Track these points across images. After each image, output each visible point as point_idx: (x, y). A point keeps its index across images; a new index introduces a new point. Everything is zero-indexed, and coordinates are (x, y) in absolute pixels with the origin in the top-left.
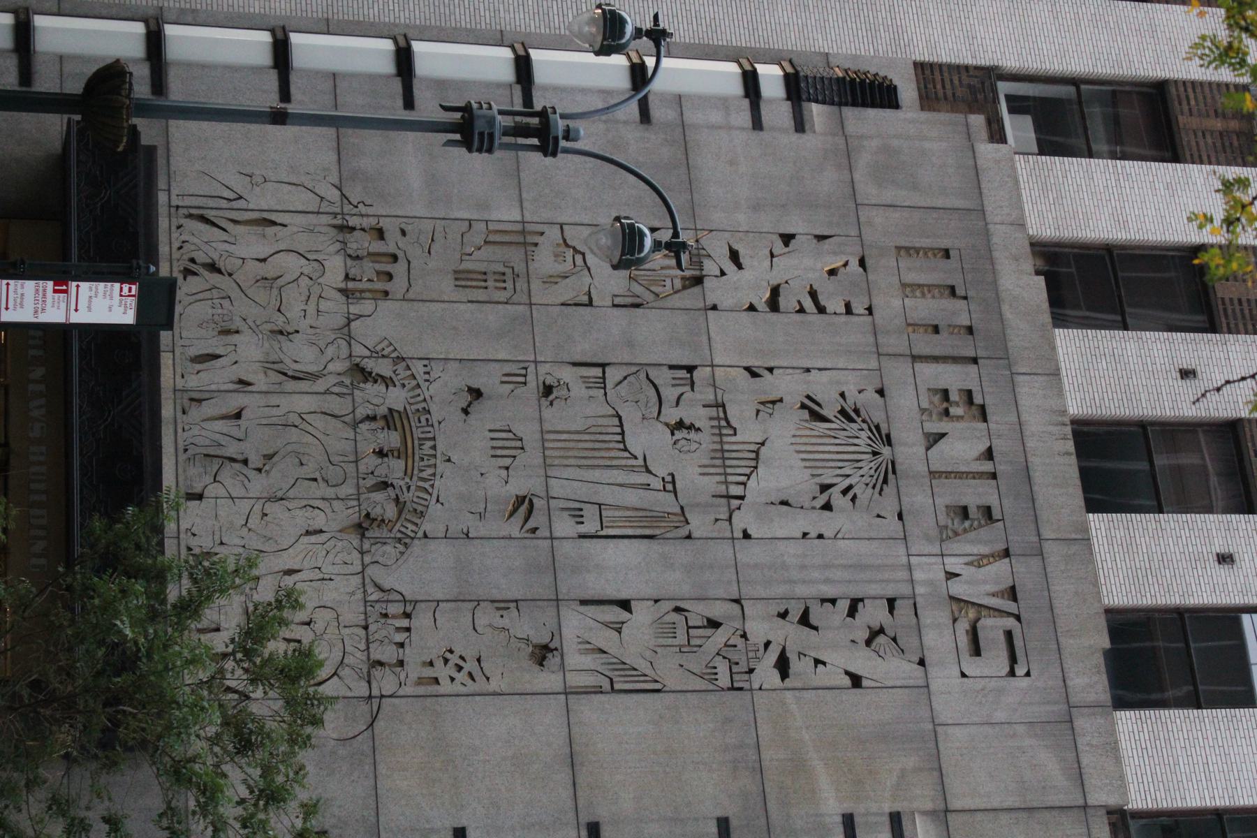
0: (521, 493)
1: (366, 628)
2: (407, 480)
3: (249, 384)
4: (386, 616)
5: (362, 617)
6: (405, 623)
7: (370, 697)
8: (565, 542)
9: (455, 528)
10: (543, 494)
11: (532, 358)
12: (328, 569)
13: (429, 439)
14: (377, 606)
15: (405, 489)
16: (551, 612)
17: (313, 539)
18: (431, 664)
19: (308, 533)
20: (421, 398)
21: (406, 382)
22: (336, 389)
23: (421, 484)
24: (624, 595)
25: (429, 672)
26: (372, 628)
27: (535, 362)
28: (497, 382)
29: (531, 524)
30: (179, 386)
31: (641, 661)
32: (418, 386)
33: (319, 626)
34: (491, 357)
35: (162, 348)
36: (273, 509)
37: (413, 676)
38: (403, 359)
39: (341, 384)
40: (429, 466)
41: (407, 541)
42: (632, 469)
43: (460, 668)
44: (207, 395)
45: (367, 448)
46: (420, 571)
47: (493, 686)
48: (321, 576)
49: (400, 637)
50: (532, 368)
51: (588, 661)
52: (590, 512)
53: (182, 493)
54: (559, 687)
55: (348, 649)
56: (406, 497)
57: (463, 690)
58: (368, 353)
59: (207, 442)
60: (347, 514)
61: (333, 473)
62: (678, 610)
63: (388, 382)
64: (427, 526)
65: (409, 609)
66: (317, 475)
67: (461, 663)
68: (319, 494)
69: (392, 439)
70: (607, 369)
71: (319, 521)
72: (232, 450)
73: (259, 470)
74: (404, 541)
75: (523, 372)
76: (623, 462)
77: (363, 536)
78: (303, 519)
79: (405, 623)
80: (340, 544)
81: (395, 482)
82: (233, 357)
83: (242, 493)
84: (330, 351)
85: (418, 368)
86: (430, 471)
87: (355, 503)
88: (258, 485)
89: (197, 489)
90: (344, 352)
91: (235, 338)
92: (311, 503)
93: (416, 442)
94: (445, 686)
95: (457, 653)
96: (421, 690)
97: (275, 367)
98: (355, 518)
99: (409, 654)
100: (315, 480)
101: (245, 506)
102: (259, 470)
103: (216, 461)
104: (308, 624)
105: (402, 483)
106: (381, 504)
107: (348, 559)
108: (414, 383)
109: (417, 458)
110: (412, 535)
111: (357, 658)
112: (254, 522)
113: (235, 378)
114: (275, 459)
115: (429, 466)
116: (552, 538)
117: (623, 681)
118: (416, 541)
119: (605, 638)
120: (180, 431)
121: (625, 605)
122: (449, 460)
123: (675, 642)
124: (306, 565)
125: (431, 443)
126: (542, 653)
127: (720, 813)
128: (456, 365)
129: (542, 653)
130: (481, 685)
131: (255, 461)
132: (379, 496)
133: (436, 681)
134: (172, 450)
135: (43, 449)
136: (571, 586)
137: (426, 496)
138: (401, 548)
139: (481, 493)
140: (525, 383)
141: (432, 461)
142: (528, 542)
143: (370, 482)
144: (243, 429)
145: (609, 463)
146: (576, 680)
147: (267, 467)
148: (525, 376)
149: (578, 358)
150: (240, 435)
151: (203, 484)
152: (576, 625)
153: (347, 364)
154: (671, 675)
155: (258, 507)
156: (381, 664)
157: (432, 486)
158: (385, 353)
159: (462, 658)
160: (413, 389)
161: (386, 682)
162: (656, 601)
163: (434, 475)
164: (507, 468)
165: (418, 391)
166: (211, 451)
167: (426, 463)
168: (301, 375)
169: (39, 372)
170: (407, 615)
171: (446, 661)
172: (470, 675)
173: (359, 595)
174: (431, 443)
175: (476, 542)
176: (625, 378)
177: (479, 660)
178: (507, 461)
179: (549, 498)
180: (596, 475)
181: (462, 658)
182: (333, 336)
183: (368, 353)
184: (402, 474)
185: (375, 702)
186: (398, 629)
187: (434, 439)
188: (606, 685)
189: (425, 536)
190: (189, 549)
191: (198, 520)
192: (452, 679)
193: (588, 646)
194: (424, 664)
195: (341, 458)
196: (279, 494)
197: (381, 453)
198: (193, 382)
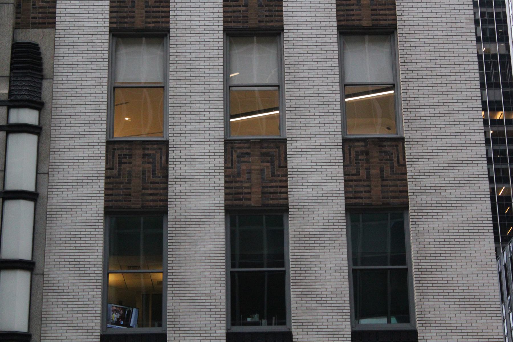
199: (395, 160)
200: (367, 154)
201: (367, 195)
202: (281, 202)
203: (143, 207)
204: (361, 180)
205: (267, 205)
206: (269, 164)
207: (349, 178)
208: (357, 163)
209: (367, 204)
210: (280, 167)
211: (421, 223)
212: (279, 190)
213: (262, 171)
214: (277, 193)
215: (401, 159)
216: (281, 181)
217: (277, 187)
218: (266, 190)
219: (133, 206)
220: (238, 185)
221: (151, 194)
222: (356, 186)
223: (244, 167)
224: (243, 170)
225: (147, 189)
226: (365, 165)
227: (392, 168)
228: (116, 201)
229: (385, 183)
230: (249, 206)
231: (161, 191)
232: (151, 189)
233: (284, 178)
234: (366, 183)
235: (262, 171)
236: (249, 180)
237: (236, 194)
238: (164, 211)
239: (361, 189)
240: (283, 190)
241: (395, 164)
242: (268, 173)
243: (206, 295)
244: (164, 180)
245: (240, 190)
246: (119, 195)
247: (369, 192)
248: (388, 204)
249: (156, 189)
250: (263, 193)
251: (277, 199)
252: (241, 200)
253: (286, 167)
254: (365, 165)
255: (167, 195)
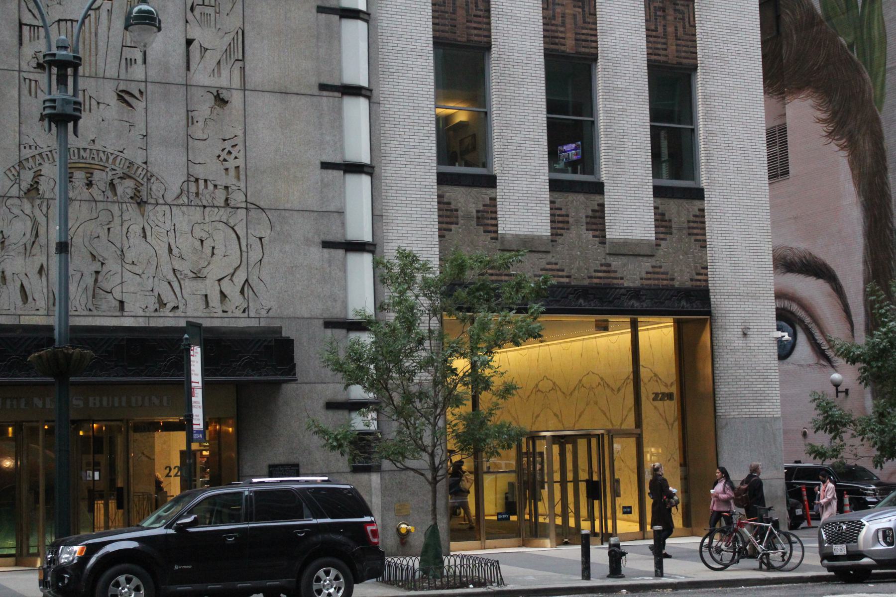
0: (116, 97)
1: (205, 207)
2: (108, 170)
3: (42, 266)
4: (197, 194)
5: (198, 208)
6: (201, 183)
7: (246, 208)
8: (149, 74)
9: (140, 143)
10: (116, 82)
11: (17, 73)
12: (168, 225)
13: (79, 152)
14: (191, 198)
15: (114, 172)
16: (193, 90)
17: (148, 234)
18: (227, 169)
19: (145, 237)
20: (49, 154)
21: (38, 162)
22: (44, 209)
23: (110, 161)
24: (184, 42)
25: (232, 172)
26: (205, 203)
27: (20, 71)
28: (35, 100)
29: (137, 95)
30: (46, 313)
31: (225, 39)
32: (40, 154)
33: (204, 235)
34: (17, 102)
35: (16, 322)
36: (130, 256)
37: (234, 181)
38: (20, 162)
39: (40, 206)
40: (98, 155)
41: (149, 175)
42: (98, 19)
43: (230, 153)
44: (51, 295)
45: (85, 193)
46: (169, 169)
47: (240, 133)
48: (172, 231)
49: (211, 187)
50: (25, 75)
51: (225, 73)
52: (128, 53)
53: (118, 314)
54: (241, 94)
55: (217, 219)
56: (119, 172)
57: (242, 152)
58: (16, 186)
59: (84, 296)
60: (132, 211)
61: (104, 217)
62: (192, 9)
63: (38, 175)
64: (139, 161)
65: (193, 179)
66: (106, 227)
67: (226, 151)
68: (119, 228)
69: (80, 176)
70: (24, 22)
71: (136, 229)
72: (90, 281)
73: (103, 264)
74: (150, 177)
75: (27, 81)
76: (93, 24)
77: (145, 202)
78: (135, 239)
79: (201, 183)
80: (152, 217)
81: (109, 178)
82: (23, 277)
83: (119, 275)
84: (16, 211)
85: (27, 153)
86: (101, 154)
87: (124, 205)
88: (113, 265)
89: (117, 304)
90: (17, 201)
91: (8, 274)
92: (124, 233)
93: (82, 161)
94: (240, 162)
95: (220, 153)
96: (242, 177)
97: (28, 248)
98: (135, 206)
99: (221, 182)
100: (109, 229)
101: (127, 275)
102: (103, 264)
103: (97, 290)
104: (202, 241)
105: (110, 174)
106: (125, 188)
107: (160, 214)
108: (38, 157)
109: (92, 162)
110: (145, 171)
111: (223, 214)
112: (136, 269)
113: (38, 276)
114: (95, 253)
115: (98, 155)
116: (146, 82)
117: (237, 52)
118: (149, 169)
119: (211, 59)
120: (76, 313)
121: (189, 42)
122: (93, 141)
123: (213, 14)
124: (166, 240)
125: (82, 151)
126: (221, 101)
127: (314, 11)
128: (23, 127)
129: (221, 101)
130: (239, 141)
131: (96, 266)
132: (120, 190)
133: (237, 168)
134: (90, 319)
135: (91, 399)
136: (177, 74)
137: (119, 158)
138: (153, 179)
139: (116, 123)
140: (36, 81)
141: (95, 152)
142: (149, 98)
143: (109, 193)
144: (74, 273)
145: (93, 35)
146: (236, 82)
147: (101, 259)
148: (30, 80)
149: (16, 41)
150: (78, 275)
151: (113, 301)
152: (202, 76)
153: (25, 200)
154: (233, 23)
155: (128, 267)
156: (227, 200)
157: (112, 154)
158: (16, 174)
159: (223, 150)
160: (42, 158)
161: (238, 198)
162: (187, 22)
163: (104, 152)
164: (98, 103)
165: (44, 155)
166: (90, 293)
167: (95, 156)
168: (34, 232)
169: (38, 402)
170: (197, 180)
171: (225, 160)
172: (233, 146)
173: (184, 209)
174: (82, 151)
175: (149, 131)
176: (30, 11)
177: (224, 140)
178: (94, 103)
179: (118, 79)
180: (102, 44)
181: (223, 150)
182: (4, 208)
183: (16, 186)
184: (104, 173)
185: (249, 206)
186: (206, 187)
187: (78, 149)
188: (240, 64)
189: (146, 163)
190: (156, 310)
191: (138, 305)
192: (236, 158)
193: (216, 71)
194: (227, 174)
195: (94, 211)
196: (119, 253)
197: (90, 184)
198: (42, 303)
199: (687, 20)
200: (664, 11)
201: (664, 52)
202: (593, 51)
203: (468, 41)
204: (658, 37)
205: (580, 53)
206: (580, 10)
207: (651, 34)
208: (656, 19)
209: (664, 62)
210: (590, 14)
211: (706, 86)
212: (589, 38)
213: (575, 15)
214: (587, 41)
215: (692, 19)
216: (591, 29)
217: (588, 34)
218: (578, 36)
219: (459, 39)
220: (553, 28)
221: (475, 28)
222: (655, 42)
223: (559, 10)
224: (558, 13)
225: (471, 22)
226: (663, 23)
227: (684, 28)
228: (443, 31)
229: (679, 42)
230: (563, 52)
231: (484, 26)
232: (475, 22)
233: (593, 26)
234: (663, 40)
235: (575, 15)
236: (563, 24)
237: (552, 37)
238: (488, 47)
239: (659, 46)
240: (593, 38)
241: (687, 24)
242: (579, 18)
243: (531, 139)
244: (487, 14)
245: (556, 34)
246: (445, 25)
247: (666, 50)
248: (681, 64)
249: (480, 23)
250: (576, 40)
251: (587, 47)
252: (557, 44)
253: (595, 15)
254: (663, 23)
255: (489, 30)
